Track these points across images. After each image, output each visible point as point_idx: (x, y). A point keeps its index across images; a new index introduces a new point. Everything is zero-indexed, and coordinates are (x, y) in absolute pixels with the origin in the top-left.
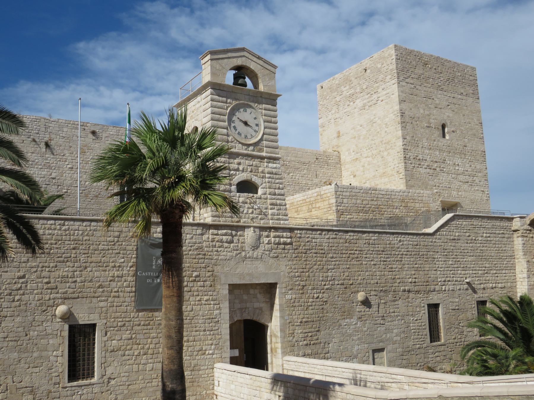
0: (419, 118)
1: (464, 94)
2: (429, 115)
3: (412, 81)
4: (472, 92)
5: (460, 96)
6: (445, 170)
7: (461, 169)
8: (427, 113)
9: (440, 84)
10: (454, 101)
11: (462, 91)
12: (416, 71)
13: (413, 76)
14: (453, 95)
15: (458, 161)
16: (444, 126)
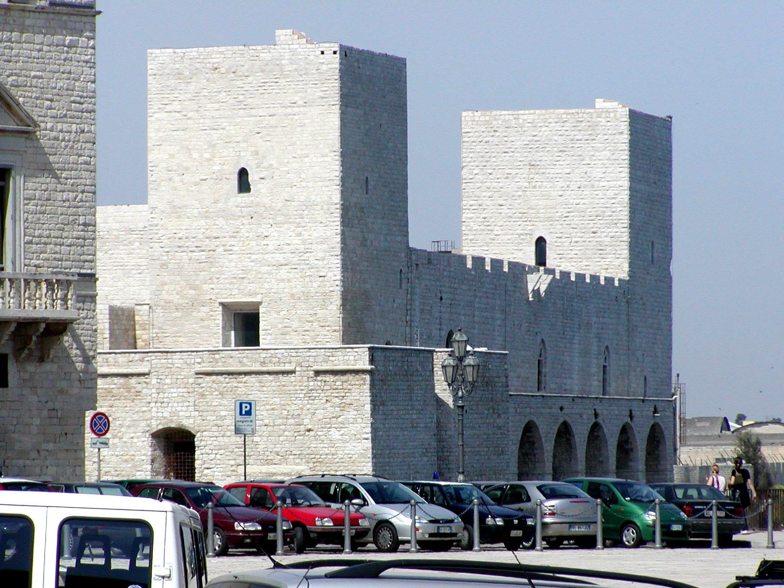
0: (187, 169)
1: (301, 102)
2: (208, 160)
3: (178, 108)
4: (321, 94)
5: (288, 110)
6: (235, 248)
7: (272, 244)
8: (207, 155)
9: (241, 98)
10: (273, 121)
11: (296, 99)
12: (192, 87)
13: (182, 97)
14: (271, 111)
15: (263, 230)
16: (243, 174)
